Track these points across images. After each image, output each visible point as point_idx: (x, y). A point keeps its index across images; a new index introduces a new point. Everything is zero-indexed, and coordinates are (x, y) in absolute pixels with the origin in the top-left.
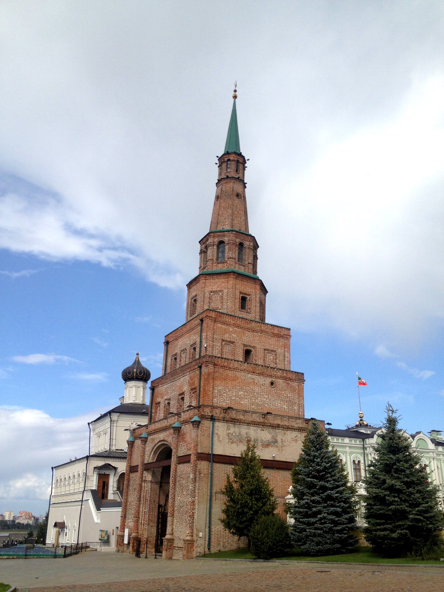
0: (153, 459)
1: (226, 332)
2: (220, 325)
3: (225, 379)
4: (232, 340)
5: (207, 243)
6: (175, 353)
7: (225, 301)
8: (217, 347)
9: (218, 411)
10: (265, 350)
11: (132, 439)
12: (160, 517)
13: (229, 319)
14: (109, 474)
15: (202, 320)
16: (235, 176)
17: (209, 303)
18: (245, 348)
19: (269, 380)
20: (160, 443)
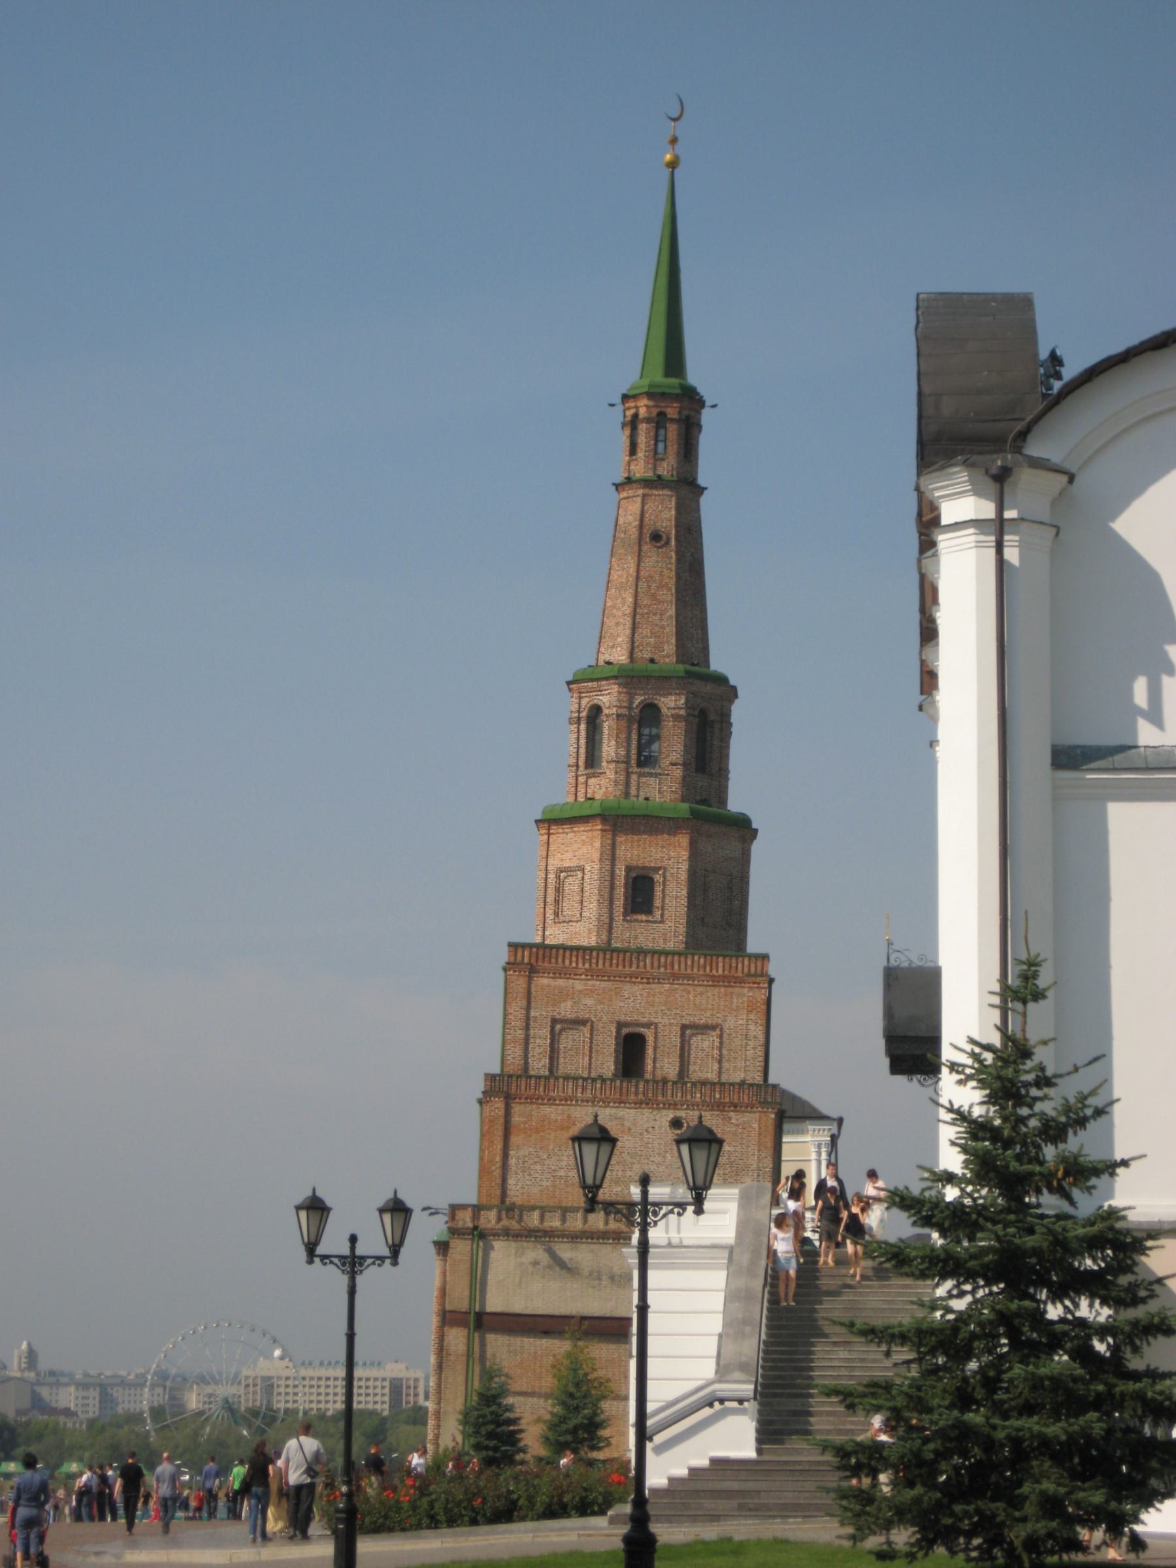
1: (563, 995)
2: (545, 981)
3: (537, 1131)
4: (582, 1015)
7: (586, 894)
8: (538, 1041)
10: (684, 1027)
13: (574, 959)
16: (650, 474)
17: (557, 902)
18: (625, 1031)
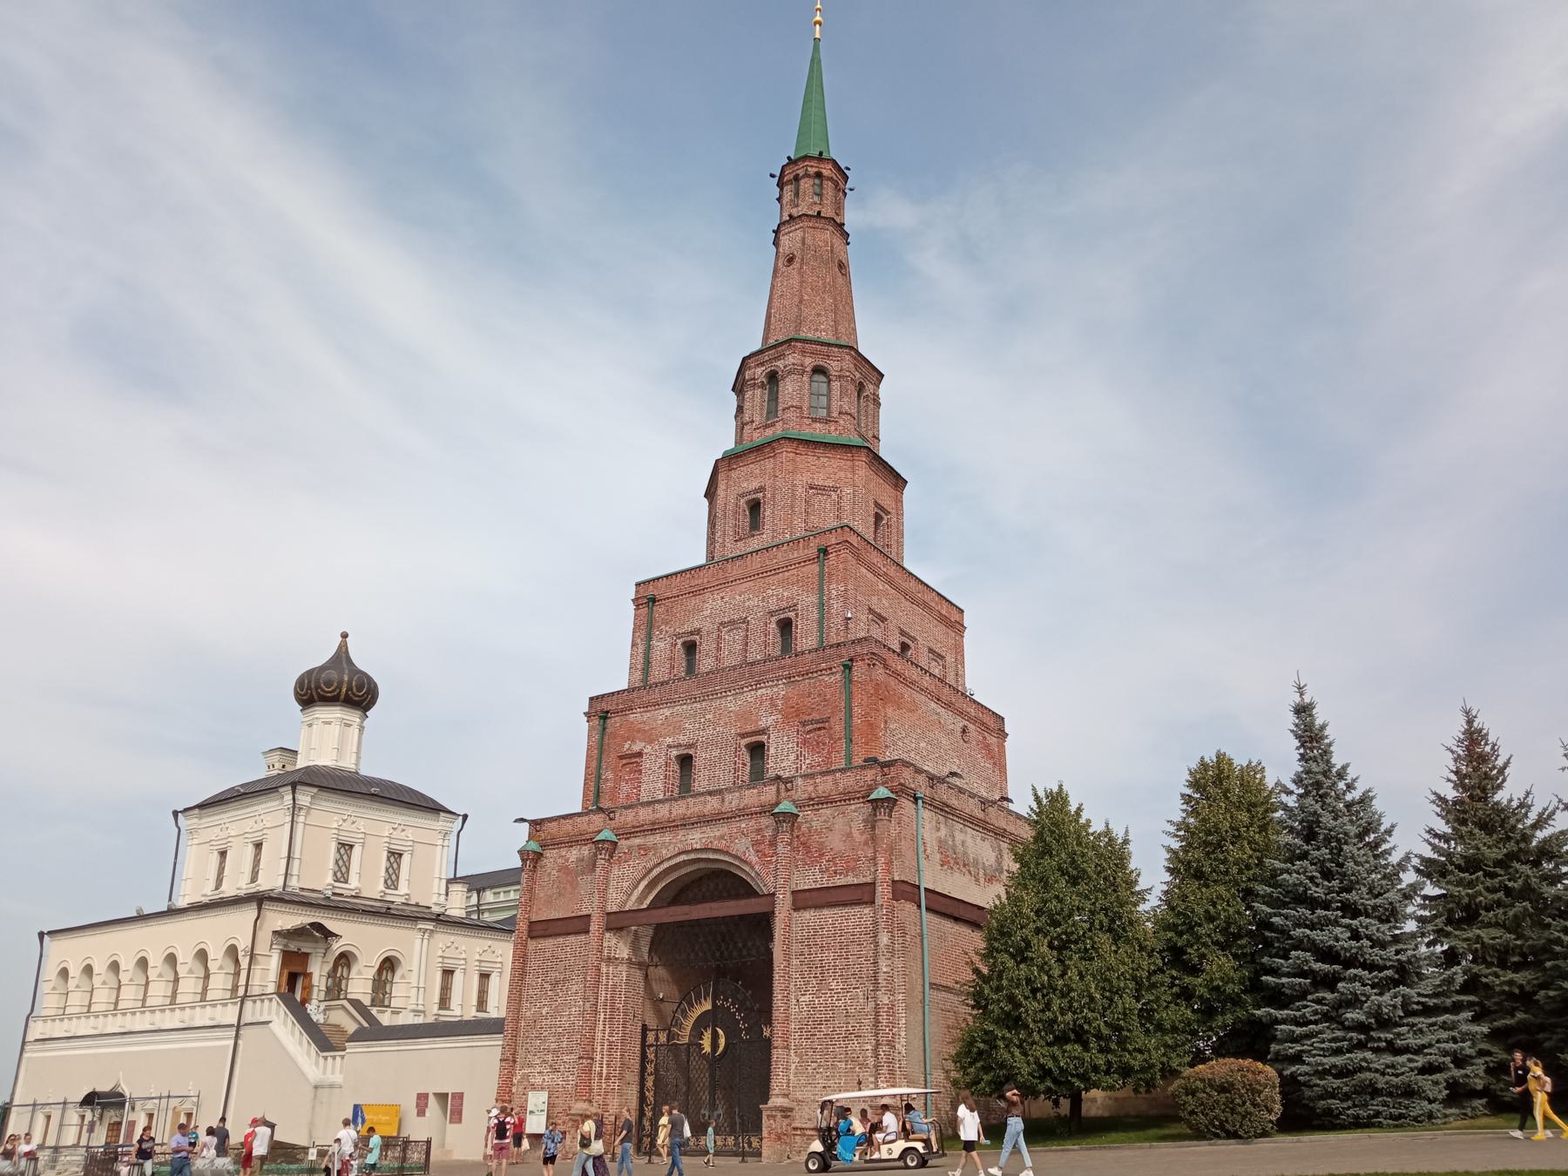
0: (641, 899)
5: (780, 364)
6: (687, 628)
9: (921, 779)
10: (931, 650)
11: (534, 846)
12: (651, 1057)
14: (307, 955)
15: (824, 551)
19: (961, 723)
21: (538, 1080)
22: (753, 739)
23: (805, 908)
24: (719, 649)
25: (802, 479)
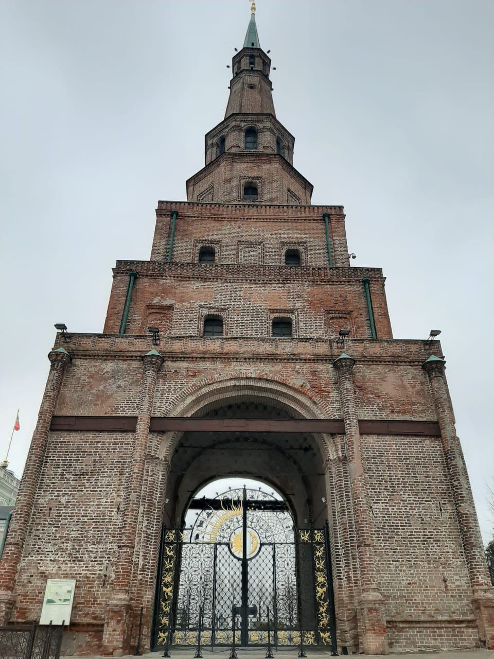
5: (260, 126)
20: (233, 383)
21: (52, 568)
22: (282, 315)
23: (368, 434)
24: (238, 257)
25: (286, 183)
